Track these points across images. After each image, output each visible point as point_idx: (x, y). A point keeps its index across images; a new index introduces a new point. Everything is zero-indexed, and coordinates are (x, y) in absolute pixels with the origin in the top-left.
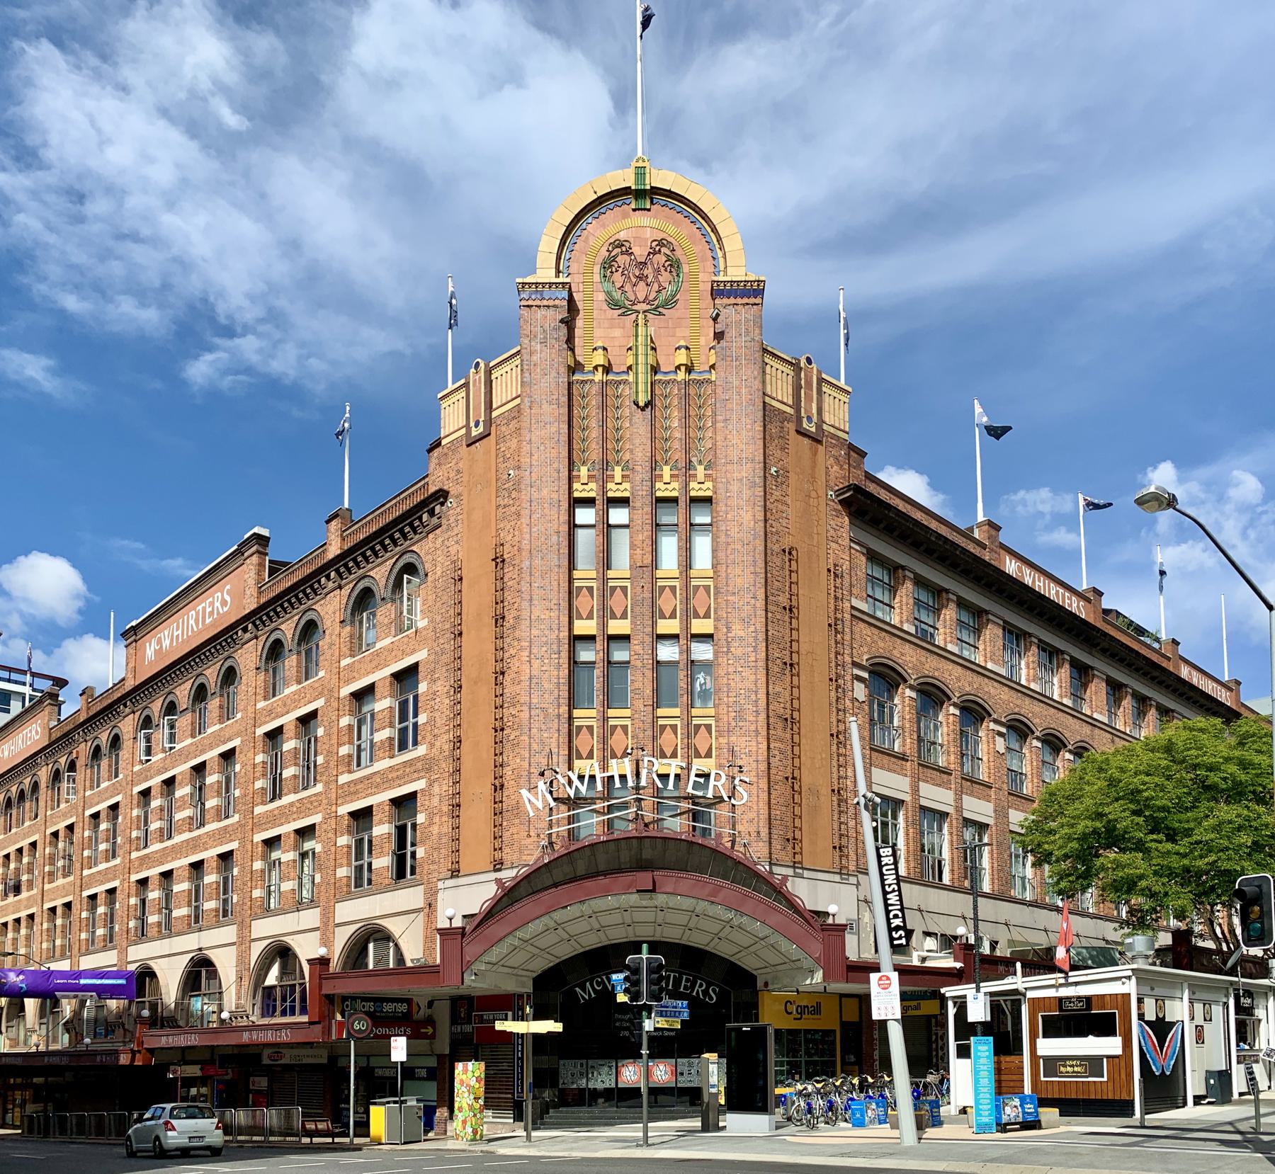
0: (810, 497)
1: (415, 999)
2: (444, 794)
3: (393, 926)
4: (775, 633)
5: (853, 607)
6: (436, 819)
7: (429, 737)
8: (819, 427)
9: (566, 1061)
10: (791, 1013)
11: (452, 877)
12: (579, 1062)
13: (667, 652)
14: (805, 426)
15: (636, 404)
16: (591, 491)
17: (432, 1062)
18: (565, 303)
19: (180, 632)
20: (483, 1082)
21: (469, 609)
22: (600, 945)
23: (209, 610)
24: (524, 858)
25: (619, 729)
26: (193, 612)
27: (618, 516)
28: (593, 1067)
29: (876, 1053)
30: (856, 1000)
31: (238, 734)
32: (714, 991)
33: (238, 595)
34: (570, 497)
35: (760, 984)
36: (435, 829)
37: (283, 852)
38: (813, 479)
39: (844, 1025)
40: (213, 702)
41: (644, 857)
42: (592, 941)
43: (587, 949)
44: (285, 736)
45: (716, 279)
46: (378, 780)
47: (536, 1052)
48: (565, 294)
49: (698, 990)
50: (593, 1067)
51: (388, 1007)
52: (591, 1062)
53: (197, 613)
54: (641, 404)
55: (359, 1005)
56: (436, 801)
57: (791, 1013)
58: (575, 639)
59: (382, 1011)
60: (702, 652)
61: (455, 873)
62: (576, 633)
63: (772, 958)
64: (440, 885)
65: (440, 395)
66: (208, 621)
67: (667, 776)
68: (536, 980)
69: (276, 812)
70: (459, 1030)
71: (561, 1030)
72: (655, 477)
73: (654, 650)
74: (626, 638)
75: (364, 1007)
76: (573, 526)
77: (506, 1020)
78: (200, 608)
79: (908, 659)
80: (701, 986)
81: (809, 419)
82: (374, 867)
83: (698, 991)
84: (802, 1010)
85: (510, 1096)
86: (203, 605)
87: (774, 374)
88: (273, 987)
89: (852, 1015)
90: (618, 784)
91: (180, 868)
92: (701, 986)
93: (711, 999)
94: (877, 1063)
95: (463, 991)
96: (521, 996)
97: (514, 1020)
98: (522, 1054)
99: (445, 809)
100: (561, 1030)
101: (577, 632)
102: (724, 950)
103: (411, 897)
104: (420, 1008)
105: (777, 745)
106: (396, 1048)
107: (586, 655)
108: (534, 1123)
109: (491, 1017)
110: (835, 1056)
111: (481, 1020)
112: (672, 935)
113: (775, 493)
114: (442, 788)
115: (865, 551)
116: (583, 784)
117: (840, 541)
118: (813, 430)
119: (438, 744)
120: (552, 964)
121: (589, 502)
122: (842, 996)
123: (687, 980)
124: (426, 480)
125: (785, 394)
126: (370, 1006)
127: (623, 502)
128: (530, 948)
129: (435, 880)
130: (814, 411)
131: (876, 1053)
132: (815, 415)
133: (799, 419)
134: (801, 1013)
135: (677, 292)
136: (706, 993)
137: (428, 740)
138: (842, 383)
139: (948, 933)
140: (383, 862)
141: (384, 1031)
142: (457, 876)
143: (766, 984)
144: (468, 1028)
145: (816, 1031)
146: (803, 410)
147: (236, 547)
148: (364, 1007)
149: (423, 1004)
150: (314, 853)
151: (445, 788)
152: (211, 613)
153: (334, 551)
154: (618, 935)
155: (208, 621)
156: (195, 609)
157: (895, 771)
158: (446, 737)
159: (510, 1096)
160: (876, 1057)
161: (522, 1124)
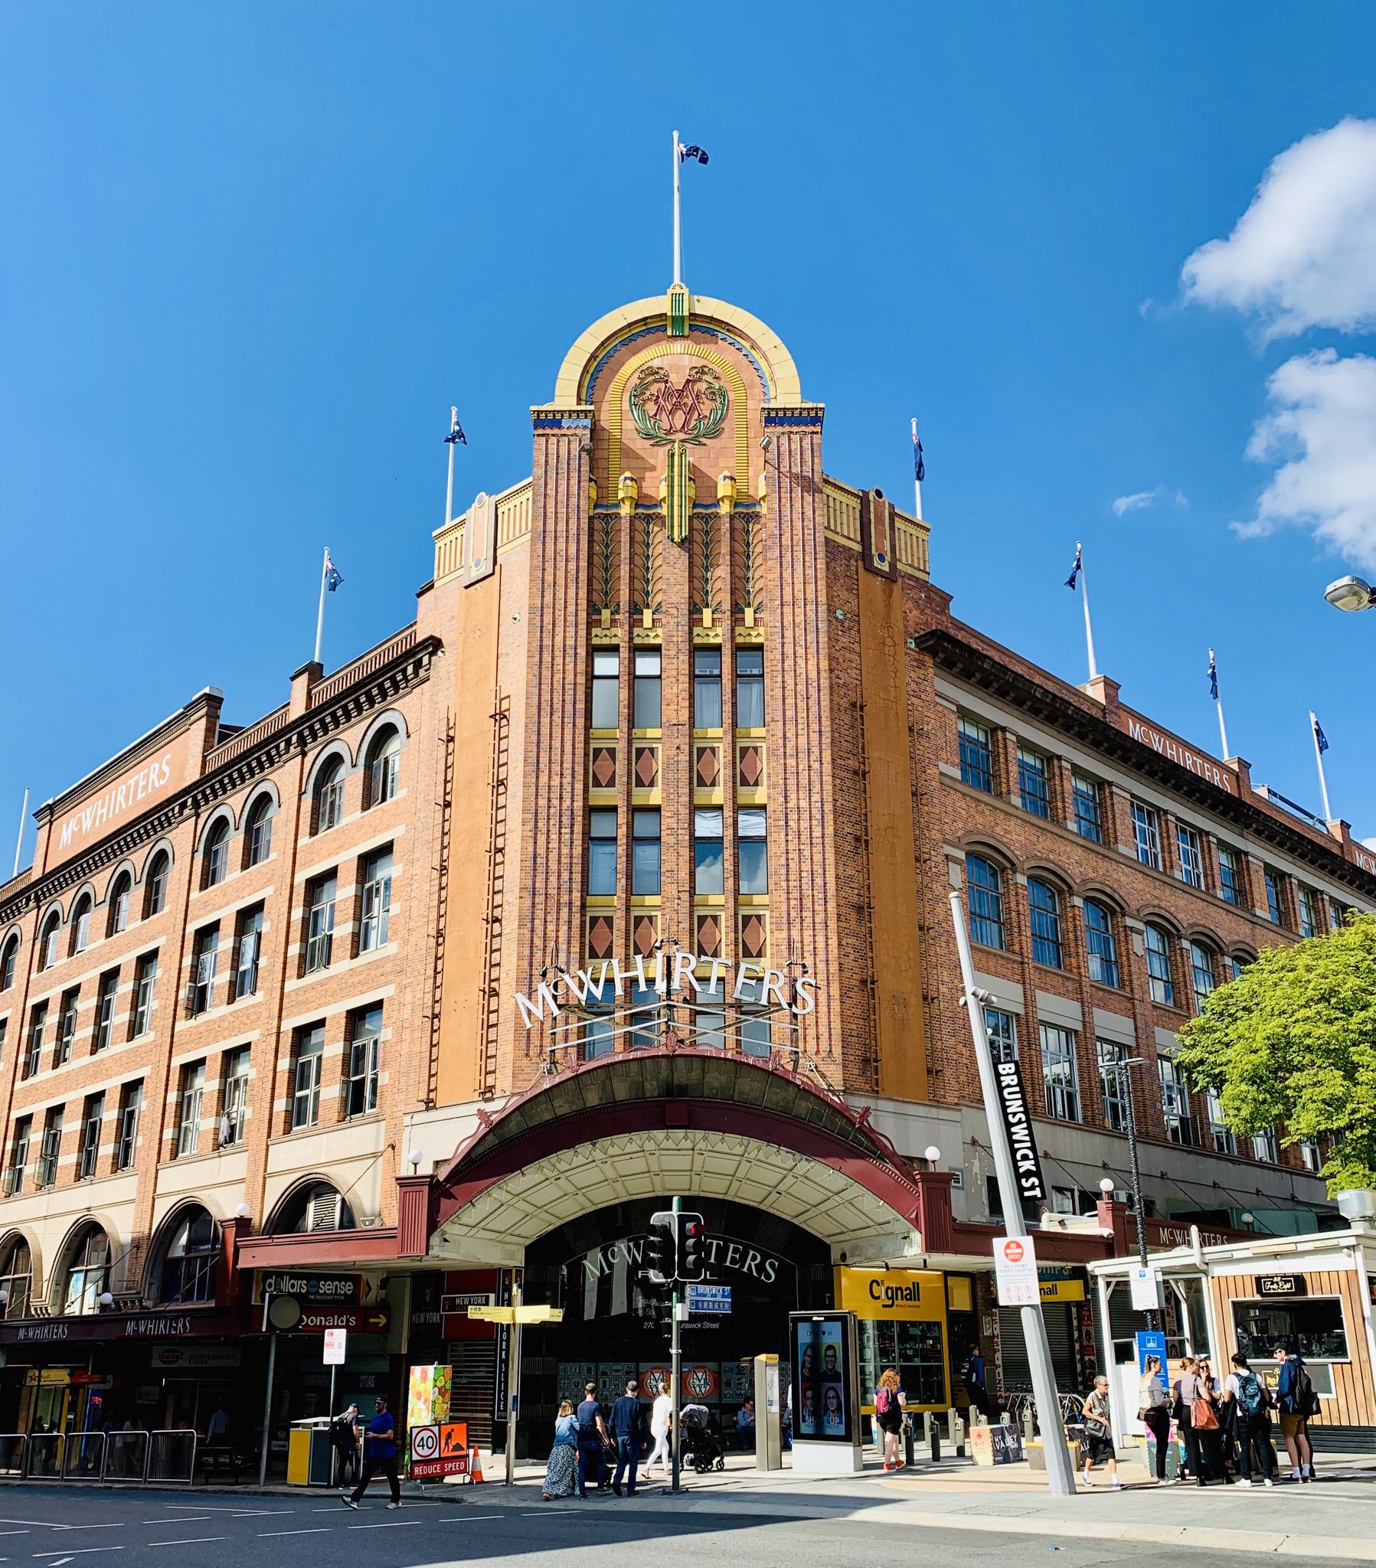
0: (884, 644)
1: (365, 1276)
2: (418, 1002)
3: (339, 1176)
4: (845, 803)
5: (941, 773)
6: (406, 1035)
7: (402, 933)
8: (893, 566)
9: (569, 1366)
10: (878, 1298)
11: (428, 1109)
12: (585, 1366)
13: (708, 826)
14: (876, 564)
15: (672, 540)
16: (619, 635)
17: (384, 1366)
18: (588, 432)
19: (105, 810)
20: (448, 1396)
21: (459, 774)
22: (617, 1201)
23: (142, 783)
24: (520, 1084)
25: (646, 921)
26: (124, 787)
27: (646, 665)
28: (605, 1373)
29: (998, 1355)
30: (966, 1282)
31: (163, 931)
32: (772, 1265)
33: (179, 766)
34: (587, 645)
35: (835, 1256)
36: (404, 1049)
37: (207, 1080)
38: (887, 623)
39: (954, 1317)
40: (137, 892)
41: (676, 1082)
42: (605, 1197)
43: (600, 1206)
44: (221, 933)
45: (766, 406)
46: (335, 986)
47: (526, 1352)
48: (587, 422)
49: (751, 1264)
50: (605, 1373)
51: (326, 1287)
52: (602, 1367)
53: (128, 789)
54: (676, 539)
55: (286, 1285)
56: (406, 1012)
57: (878, 1298)
58: (591, 810)
59: (317, 1293)
60: (751, 825)
61: (430, 1104)
62: (591, 803)
63: (852, 1220)
64: (407, 1120)
65: (435, 533)
66: (140, 796)
67: (708, 979)
68: (529, 1249)
69: (202, 1029)
70: (422, 1320)
71: (560, 1320)
72: (694, 619)
73: (692, 823)
74: (657, 809)
75: (293, 1286)
76: (591, 677)
77: (487, 1304)
78: (132, 782)
79: (1015, 837)
80: (754, 1258)
81: (881, 557)
82: (321, 1098)
83: (750, 1265)
84: (894, 1294)
85: (487, 1415)
86: (137, 777)
87: (838, 508)
88: (181, 1259)
89: (962, 1301)
90: (643, 987)
91: (74, 1101)
92: (754, 1258)
93: (768, 1276)
94: (1000, 1370)
95: (428, 1263)
96: (508, 1272)
97: (497, 1304)
98: (507, 1355)
99: (418, 1021)
100: (560, 1320)
101: (593, 802)
102: (785, 1209)
103: (363, 1135)
104: (370, 1289)
105: (849, 941)
106: (331, 1345)
107: (601, 827)
108: (518, 1456)
109: (466, 1302)
110: (941, 1360)
111: (452, 1305)
112: (714, 1188)
113: (842, 639)
114: (418, 995)
115: (954, 708)
116: (597, 986)
117: (923, 697)
118: (886, 568)
119: (413, 940)
120: (551, 1228)
121: (614, 649)
122: (947, 1274)
123: (735, 1251)
124: (414, 628)
125: (852, 529)
126: (301, 1286)
127: (656, 649)
128: (522, 1205)
129: (401, 1114)
130: (887, 548)
131: (998, 1355)
132: (889, 553)
133: (865, 556)
134: (892, 1298)
135: (722, 419)
136: (761, 1268)
137: (400, 935)
138: (919, 517)
139: (1088, 1189)
140: (331, 1091)
141: (318, 1320)
142: (434, 1107)
143: (844, 1257)
144: (434, 1318)
145: (914, 1324)
146: (873, 547)
147: (182, 710)
148: (293, 1286)
149: (375, 1284)
150: (246, 1081)
151: (419, 995)
152: (145, 787)
153: (297, 710)
154: (641, 1188)
155: (140, 796)
156: (125, 783)
157: (1004, 977)
158: (424, 931)
159: (487, 1415)
160: (999, 1362)
161: (504, 1457)
